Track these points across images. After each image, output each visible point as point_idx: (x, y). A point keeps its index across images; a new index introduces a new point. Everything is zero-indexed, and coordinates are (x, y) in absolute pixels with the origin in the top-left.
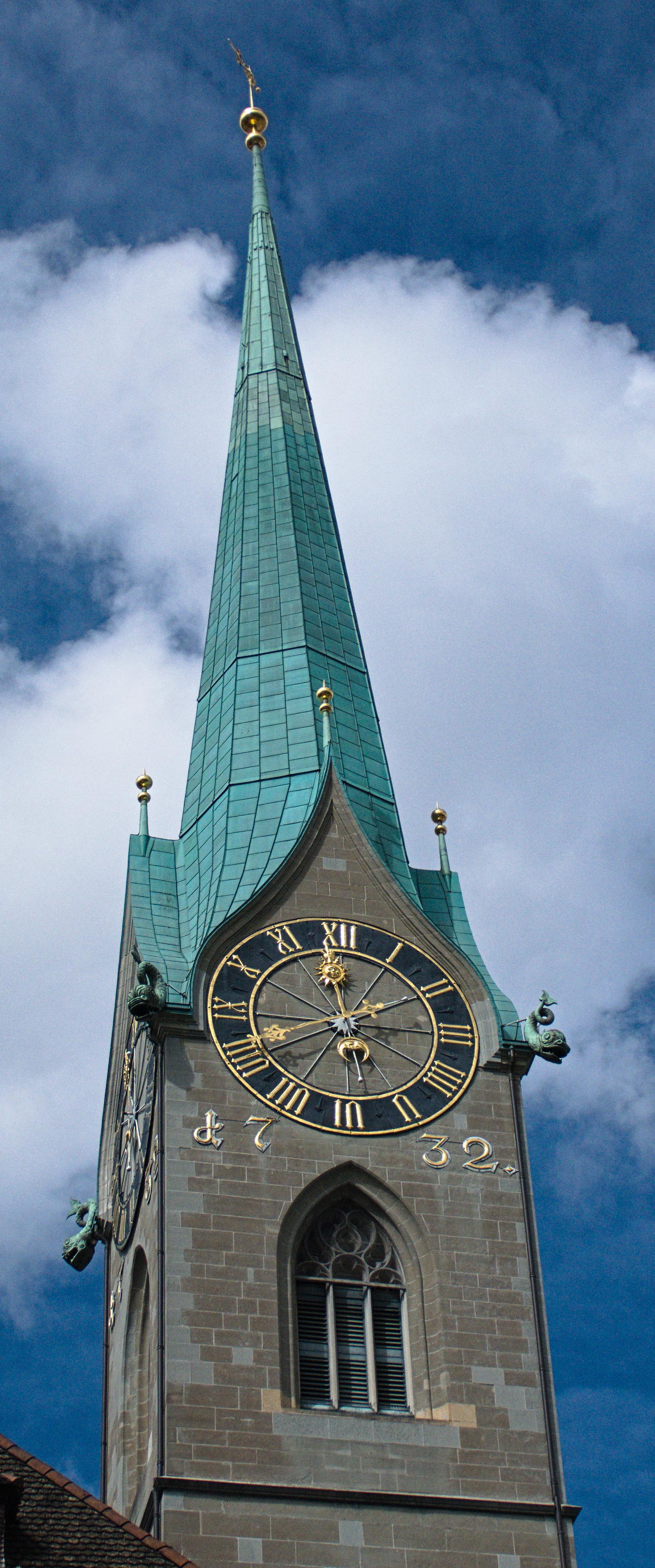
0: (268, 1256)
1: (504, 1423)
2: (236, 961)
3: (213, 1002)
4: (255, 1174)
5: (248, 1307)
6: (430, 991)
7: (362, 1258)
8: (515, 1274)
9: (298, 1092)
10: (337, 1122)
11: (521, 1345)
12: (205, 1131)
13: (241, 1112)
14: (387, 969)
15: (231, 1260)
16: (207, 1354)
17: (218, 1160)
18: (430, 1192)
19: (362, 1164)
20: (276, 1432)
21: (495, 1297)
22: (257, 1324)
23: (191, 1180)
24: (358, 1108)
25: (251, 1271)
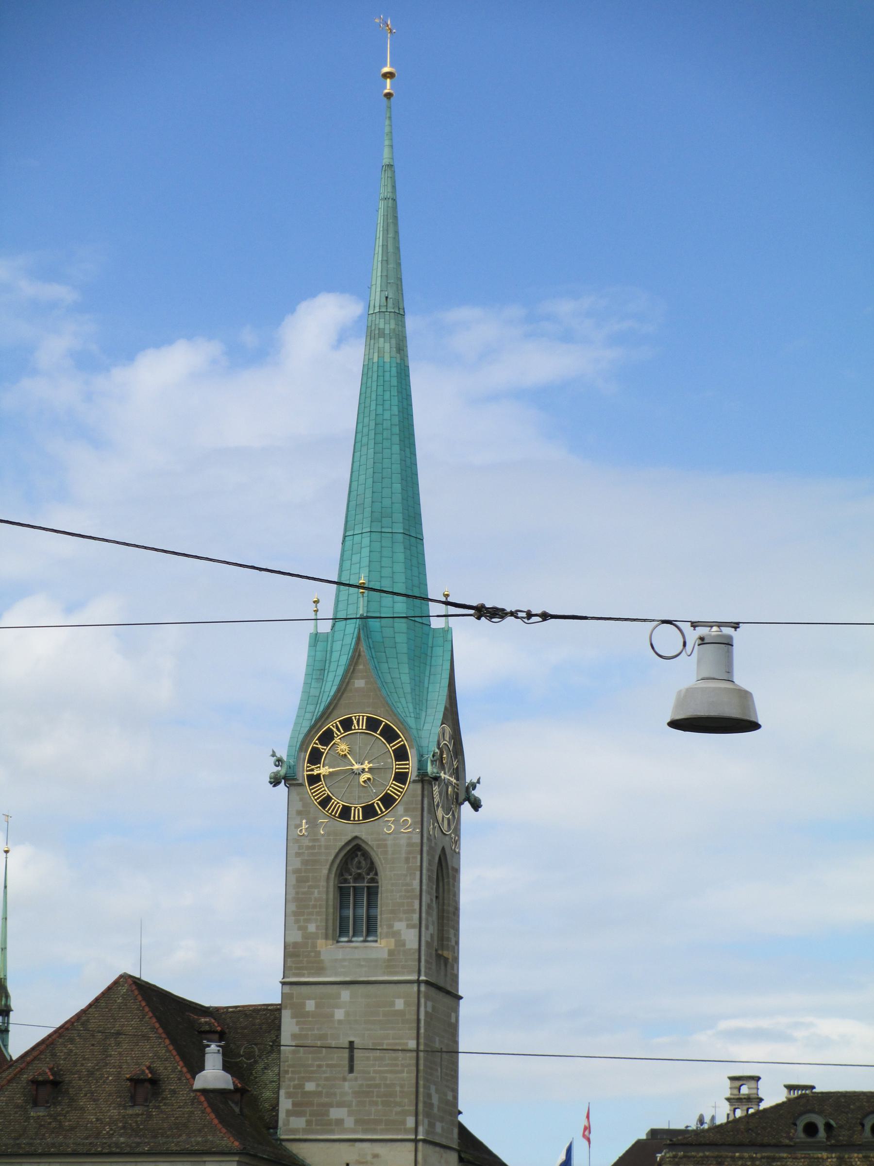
0: (323, 883)
1: (404, 945)
2: (317, 744)
3: (307, 767)
4: (320, 846)
5: (314, 906)
6: (394, 746)
7: (364, 873)
8: (415, 880)
9: (338, 805)
10: (352, 819)
11: (413, 911)
12: (301, 830)
13: (316, 819)
14: (377, 737)
15: (309, 887)
16: (300, 928)
17: (306, 842)
18: (385, 846)
19: (360, 836)
20: (322, 958)
21: (407, 891)
23: (297, 853)
24: (360, 809)
25: (316, 891)
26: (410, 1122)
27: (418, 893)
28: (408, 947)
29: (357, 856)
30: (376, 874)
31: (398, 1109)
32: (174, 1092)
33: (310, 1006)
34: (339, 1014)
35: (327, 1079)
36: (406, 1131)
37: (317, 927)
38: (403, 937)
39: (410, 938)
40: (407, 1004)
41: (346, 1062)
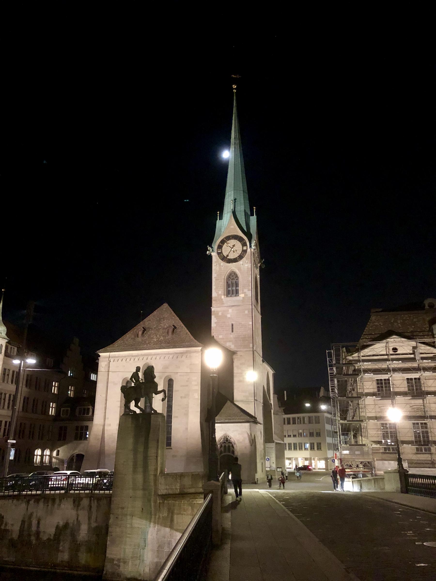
15: (219, 281)
16: (216, 293)
18: (241, 269)
22: (222, 288)
25: (221, 282)
26: (251, 345)
27: (251, 281)
28: (248, 296)
29: (232, 273)
30: (238, 278)
31: (247, 342)
32: (180, 332)
33: (220, 314)
34: (229, 316)
35: (225, 334)
36: (250, 348)
37: (222, 292)
38: (247, 293)
39: (249, 294)
40: (248, 312)
41: (231, 329)
